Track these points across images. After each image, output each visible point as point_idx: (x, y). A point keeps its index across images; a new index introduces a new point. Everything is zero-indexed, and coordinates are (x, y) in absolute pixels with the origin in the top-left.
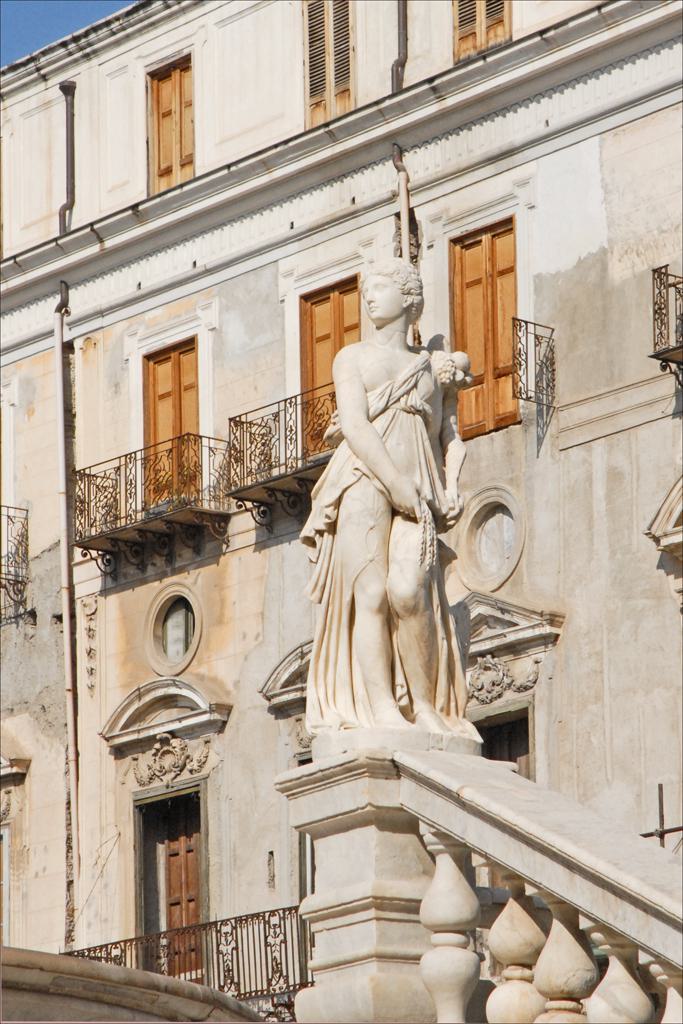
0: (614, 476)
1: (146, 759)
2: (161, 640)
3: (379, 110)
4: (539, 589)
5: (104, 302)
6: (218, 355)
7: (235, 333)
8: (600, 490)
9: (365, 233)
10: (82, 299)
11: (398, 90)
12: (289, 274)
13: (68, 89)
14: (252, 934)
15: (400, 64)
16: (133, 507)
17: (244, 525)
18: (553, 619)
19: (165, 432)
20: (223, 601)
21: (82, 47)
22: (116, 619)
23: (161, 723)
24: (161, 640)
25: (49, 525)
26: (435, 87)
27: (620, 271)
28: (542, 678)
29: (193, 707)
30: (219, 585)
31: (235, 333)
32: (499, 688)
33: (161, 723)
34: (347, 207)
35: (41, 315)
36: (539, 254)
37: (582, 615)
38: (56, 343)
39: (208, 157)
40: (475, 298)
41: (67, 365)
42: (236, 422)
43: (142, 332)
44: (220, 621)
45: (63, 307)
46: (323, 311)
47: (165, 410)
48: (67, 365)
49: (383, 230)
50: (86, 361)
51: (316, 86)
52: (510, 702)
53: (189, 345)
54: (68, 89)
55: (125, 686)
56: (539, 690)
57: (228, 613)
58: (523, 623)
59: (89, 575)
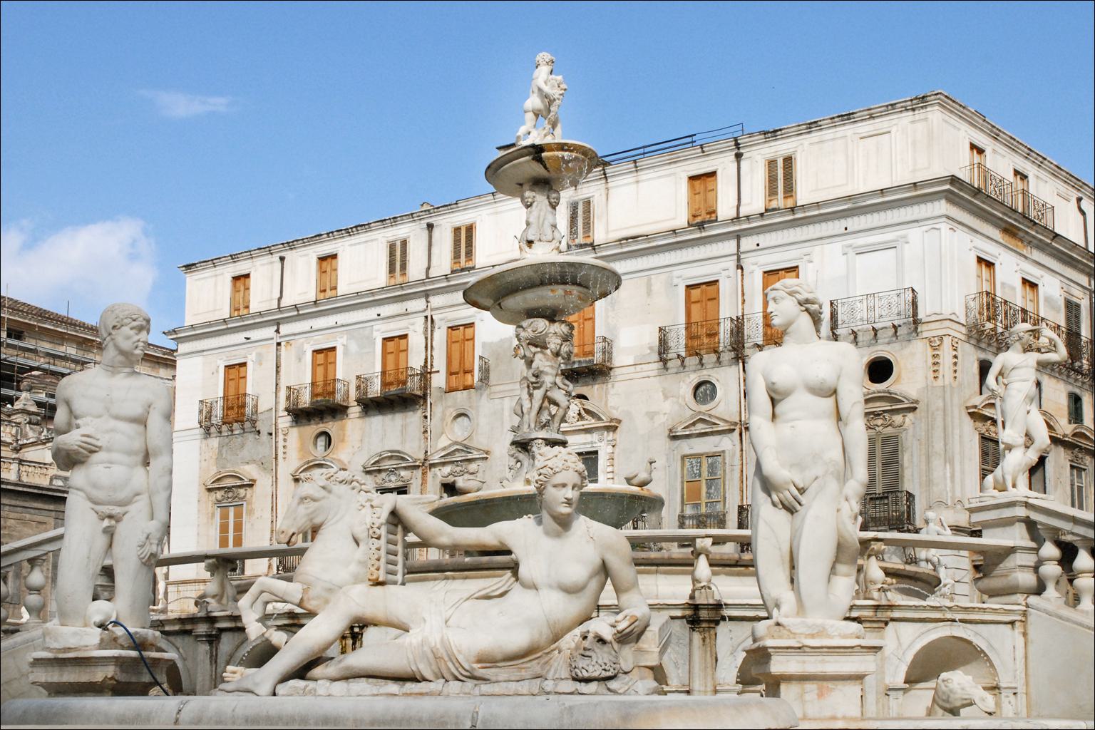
3: (423, 282)
4: (480, 441)
5: (296, 331)
6: (346, 353)
7: (353, 347)
9: (412, 321)
10: (285, 329)
11: (427, 277)
12: (378, 330)
13: (282, 259)
15: (429, 268)
16: (305, 400)
17: (355, 410)
18: (487, 453)
19: (320, 378)
20: (344, 435)
21: (290, 245)
28: (481, 471)
30: (343, 429)
34: (404, 311)
35: (269, 332)
39: (343, 289)
40: (456, 347)
42: (358, 377)
43: (312, 343)
44: (343, 441)
45: (277, 331)
46: (390, 344)
47: (320, 370)
50: (286, 350)
51: (392, 270)
53: (333, 349)
55: (300, 459)
57: (346, 439)
58: (475, 453)
59: (285, 421)
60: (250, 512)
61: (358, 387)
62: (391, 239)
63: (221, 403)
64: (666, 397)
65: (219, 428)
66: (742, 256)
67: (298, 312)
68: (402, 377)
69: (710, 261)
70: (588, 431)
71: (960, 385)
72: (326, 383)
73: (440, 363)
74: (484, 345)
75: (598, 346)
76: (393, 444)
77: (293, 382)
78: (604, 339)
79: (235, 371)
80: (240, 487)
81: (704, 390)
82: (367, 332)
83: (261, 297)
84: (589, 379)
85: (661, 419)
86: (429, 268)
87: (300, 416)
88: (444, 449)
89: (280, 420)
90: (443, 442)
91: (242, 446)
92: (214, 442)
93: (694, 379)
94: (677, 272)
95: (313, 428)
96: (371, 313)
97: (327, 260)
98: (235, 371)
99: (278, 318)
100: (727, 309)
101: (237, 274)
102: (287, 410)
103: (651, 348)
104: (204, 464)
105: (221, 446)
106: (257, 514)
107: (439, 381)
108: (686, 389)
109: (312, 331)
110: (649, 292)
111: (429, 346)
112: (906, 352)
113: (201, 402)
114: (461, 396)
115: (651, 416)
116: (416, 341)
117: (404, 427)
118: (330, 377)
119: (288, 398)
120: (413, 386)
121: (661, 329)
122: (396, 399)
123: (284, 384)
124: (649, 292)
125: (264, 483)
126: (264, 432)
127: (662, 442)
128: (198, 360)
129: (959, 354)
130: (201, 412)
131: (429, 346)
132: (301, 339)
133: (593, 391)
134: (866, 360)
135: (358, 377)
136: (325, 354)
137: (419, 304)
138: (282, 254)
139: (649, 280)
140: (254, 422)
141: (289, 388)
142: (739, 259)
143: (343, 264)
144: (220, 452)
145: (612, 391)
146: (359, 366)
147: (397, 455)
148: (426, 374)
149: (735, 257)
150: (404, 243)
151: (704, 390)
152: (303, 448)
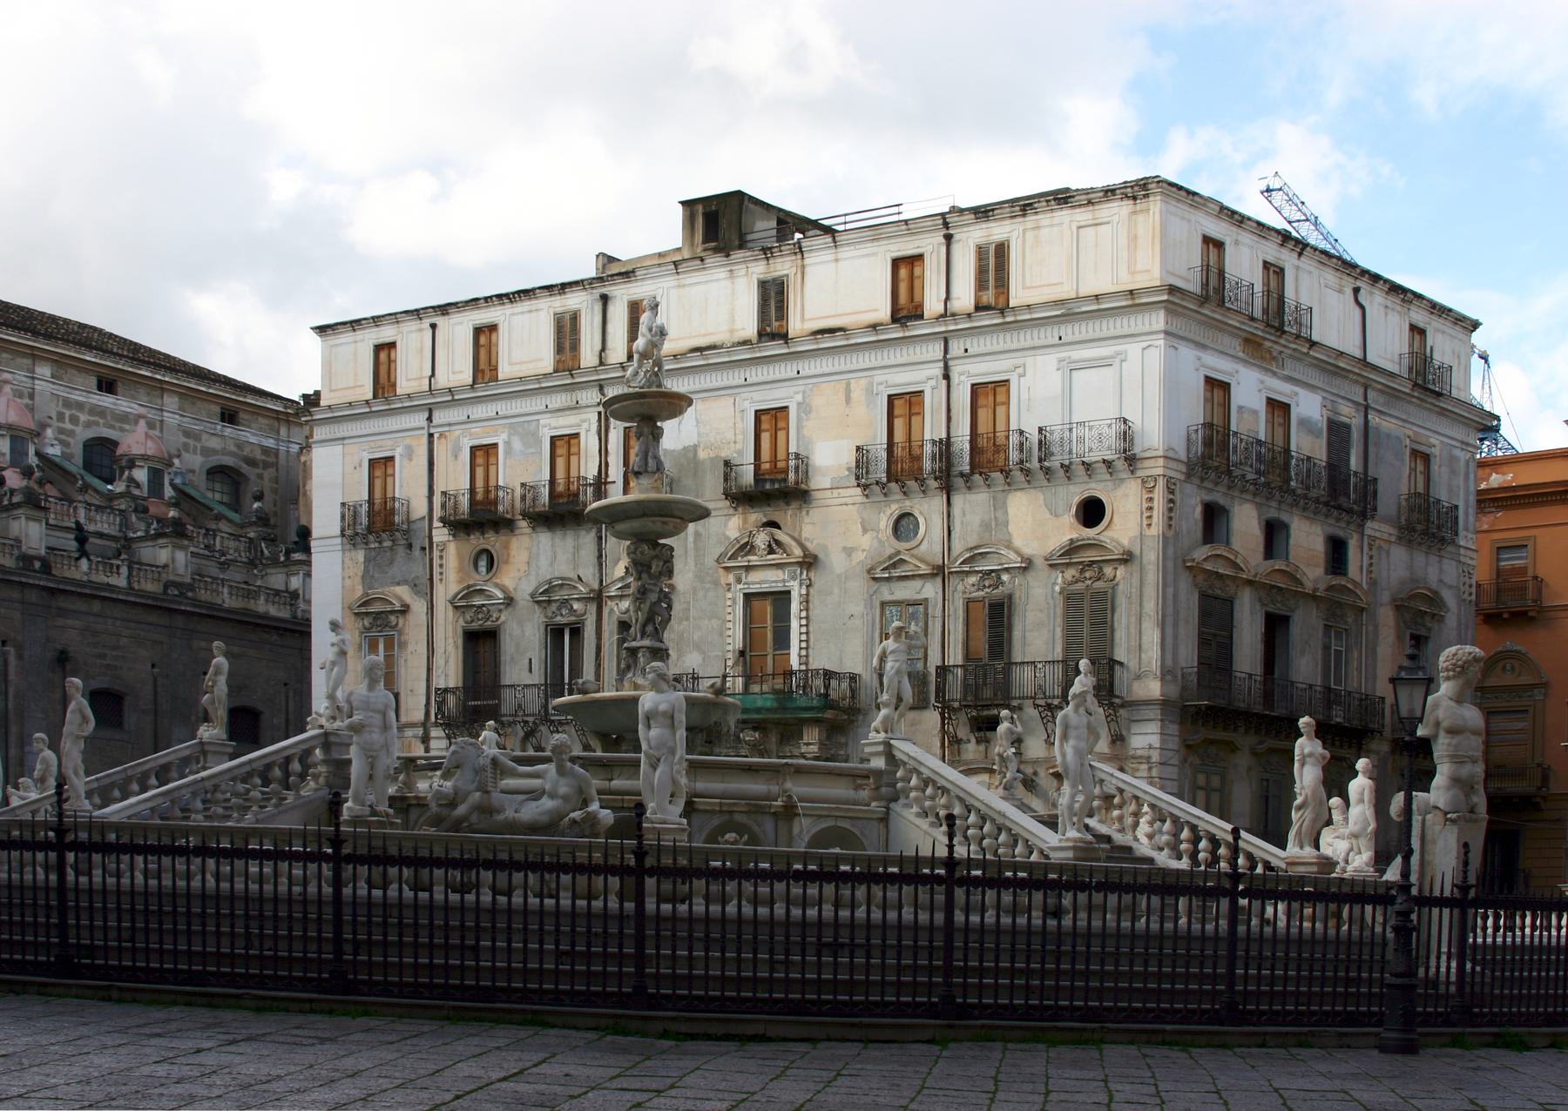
3: (595, 370)
6: (508, 452)
7: (517, 445)
9: (584, 416)
11: (601, 363)
13: (433, 326)
15: (603, 349)
22: (451, 555)
25: (419, 508)
27: (702, 455)
29: (490, 597)
30: (506, 547)
31: (517, 445)
35: (420, 419)
38: (425, 432)
42: (523, 485)
45: (430, 419)
55: (460, 582)
59: (441, 534)
60: (403, 645)
61: (523, 498)
63: (365, 507)
64: (865, 531)
65: (365, 536)
66: (951, 363)
67: (453, 397)
68: (574, 487)
69: (913, 367)
70: (779, 566)
71: (1177, 534)
72: (487, 491)
75: (792, 463)
76: (564, 569)
77: (451, 488)
78: (797, 456)
79: (381, 466)
80: (392, 612)
81: (903, 525)
82: (532, 427)
83: (410, 376)
85: (859, 556)
86: (603, 349)
87: (460, 527)
89: (434, 532)
91: (391, 562)
92: (360, 555)
93: (894, 509)
94: (879, 377)
96: (537, 404)
98: (381, 466)
99: (433, 402)
100: (932, 428)
101: (381, 341)
102: (442, 520)
103: (849, 469)
104: (348, 582)
105: (367, 560)
106: (410, 648)
108: (885, 522)
109: (469, 421)
110: (848, 400)
111: (603, 451)
112: (1120, 492)
115: (849, 551)
117: (577, 548)
119: (443, 506)
121: (858, 448)
123: (439, 487)
124: (848, 400)
125: (419, 607)
127: (859, 585)
128: (337, 449)
129: (1178, 497)
130: (343, 517)
131: (603, 451)
132: (457, 431)
133: (786, 515)
134: (1076, 500)
135: (523, 485)
136: (483, 454)
138: (433, 320)
139: (848, 385)
140: (407, 532)
141: (444, 493)
142: (946, 367)
143: (503, 339)
144: (366, 570)
145: (807, 520)
146: (522, 472)
147: (565, 583)
149: (941, 364)
151: (903, 525)
152: (461, 569)
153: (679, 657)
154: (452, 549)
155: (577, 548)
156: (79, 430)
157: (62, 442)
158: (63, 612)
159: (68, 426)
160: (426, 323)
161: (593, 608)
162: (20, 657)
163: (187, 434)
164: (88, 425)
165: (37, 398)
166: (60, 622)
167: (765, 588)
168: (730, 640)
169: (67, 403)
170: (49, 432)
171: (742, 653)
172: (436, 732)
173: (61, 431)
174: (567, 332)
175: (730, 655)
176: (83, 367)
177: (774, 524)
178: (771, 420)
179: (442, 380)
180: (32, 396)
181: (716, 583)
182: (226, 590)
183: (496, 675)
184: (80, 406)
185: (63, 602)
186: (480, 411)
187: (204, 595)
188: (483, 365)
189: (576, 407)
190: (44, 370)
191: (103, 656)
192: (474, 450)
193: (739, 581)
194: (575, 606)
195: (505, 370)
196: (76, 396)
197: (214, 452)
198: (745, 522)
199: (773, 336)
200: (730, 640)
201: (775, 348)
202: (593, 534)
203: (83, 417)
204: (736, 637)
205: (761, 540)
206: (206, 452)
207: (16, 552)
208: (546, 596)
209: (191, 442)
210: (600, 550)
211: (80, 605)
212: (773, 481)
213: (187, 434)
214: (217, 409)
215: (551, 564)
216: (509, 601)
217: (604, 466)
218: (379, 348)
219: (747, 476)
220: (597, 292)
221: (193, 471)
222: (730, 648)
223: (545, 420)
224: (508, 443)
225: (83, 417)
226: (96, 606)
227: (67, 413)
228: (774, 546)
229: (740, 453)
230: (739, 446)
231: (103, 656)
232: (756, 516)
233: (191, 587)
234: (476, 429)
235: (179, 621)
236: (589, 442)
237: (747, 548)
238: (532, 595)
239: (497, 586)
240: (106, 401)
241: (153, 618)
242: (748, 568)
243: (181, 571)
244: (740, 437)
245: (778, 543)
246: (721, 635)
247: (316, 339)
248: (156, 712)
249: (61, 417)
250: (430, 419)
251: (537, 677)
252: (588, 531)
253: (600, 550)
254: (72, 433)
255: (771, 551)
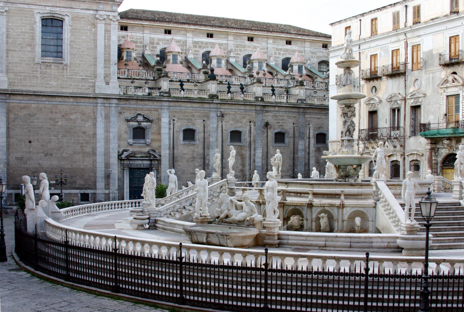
0: (433, 78)
1: (370, 106)
2: (372, 91)
3: (403, 29)
4: (423, 90)
6: (380, 56)
7: (383, 54)
8: (431, 79)
9: (401, 43)
11: (405, 26)
14: (385, 130)
15: (406, 22)
17: (384, 78)
23: (372, 102)
24: (372, 91)
26: (411, 27)
27: (434, 52)
29: (376, 100)
30: (380, 85)
32: (417, 102)
33: (372, 102)
36: (424, 48)
37: (428, 94)
38: (358, 52)
39: (380, 31)
41: (360, 55)
44: (380, 90)
45: (359, 48)
48: (360, 55)
49: (403, 43)
51: (394, 23)
52: (418, 104)
54: (360, 20)
56: (422, 103)
59: (362, 82)
62: (394, 11)
67: (365, 41)
68: (398, 65)
73: (410, 60)
74: (423, 52)
76: (396, 91)
82: (387, 47)
84: (457, 66)
86: (406, 22)
87: (368, 80)
88: (411, 93)
89: (361, 82)
90: (411, 90)
95: (372, 83)
96: (388, 41)
97: (374, 20)
107: (409, 66)
109: (370, 48)
111: (406, 54)
113: (336, 76)
114: (416, 72)
116: (402, 51)
117: (399, 84)
118: (376, 66)
120: (402, 69)
122: (396, 73)
126: (356, 87)
131: (406, 54)
136: (374, 57)
137: (403, 37)
143: (379, 21)
148: (405, 64)
150: (398, 13)
153: (427, 117)
154: (365, 86)
155: (399, 84)
156: (280, 56)
157: (275, 60)
158: (267, 111)
159: (277, 56)
160: (359, 19)
161: (403, 102)
162: (255, 125)
163: (312, 53)
164: (283, 54)
165: (268, 49)
166: (266, 114)
167: (452, 94)
168: (442, 111)
169: (277, 49)
170: (272, 58)
171: (446, 115)
172: (360, 142)
173: (276, 57)
174: (396, 17)
175: (442, 116)
176: (281, 38)
177: (454, 73)
178: (454, 39)
179: (363, 36)
180: (267, 49)
181: (438, 93)
182: (316, 99)
183: (377, 125)
184: (281, 50)
185: (267, 109)
186: (373, 44)
187: (309, 102)
188: (374, 30)
189: (398, 41)
190: (271, 41)
191: (279, 123)
192: (371, 56)
193: (444, 92)
194: (399, 102)
195: (379, 32)
196: (280, 47)
197: (321, 57)
198: (446, 73)
199: (455, 13)
200: (442, 111)
201: (455, 16)
202: (404, 78)
203: (282, 53)
204: (444, 110)
205: (450, 78)
206: (318, 57)
207: (254, 96)
208: (390, 100)
209: (314, 55)
210: (405, 84)
211: (272, 109)
212: (455, 59)
213: (312, 53)
214: (322, 45)
215: (392, 90)
216: (380, 102)
217: (406, 58)
218: (346, 28)
219: (447, 59)
220: (359, 19)
221: (314, 63)
222: (442, 113)
223: (390, 45)
224: (380, 53)
225: (282, 53)
226: (277, 109)
227: (277, 52)
228: (454, 80)
229: (445, 51)
230: (445, 49)
231: (279, 123)
232: (450, 70)
233: (305, 100)
234: (372, 50)
235: (301, 110)
236: (402, 51)
237: (446, 81)
238: (386, 99)
239: (377, 97)
240: (289, 47)
241: (294, 110)
242: (447, 88)
243: (302, 95)
244: (445, 46)
245: (455, 79)
246: (439, 109)
247: (330, 26)
248: (294, 137)
249: (275, 53)
250: (359, 48)
251: (388, 125)
252: (402, 79)
253: (405, 84)
254: (278, 58)
255: (453, 82)
